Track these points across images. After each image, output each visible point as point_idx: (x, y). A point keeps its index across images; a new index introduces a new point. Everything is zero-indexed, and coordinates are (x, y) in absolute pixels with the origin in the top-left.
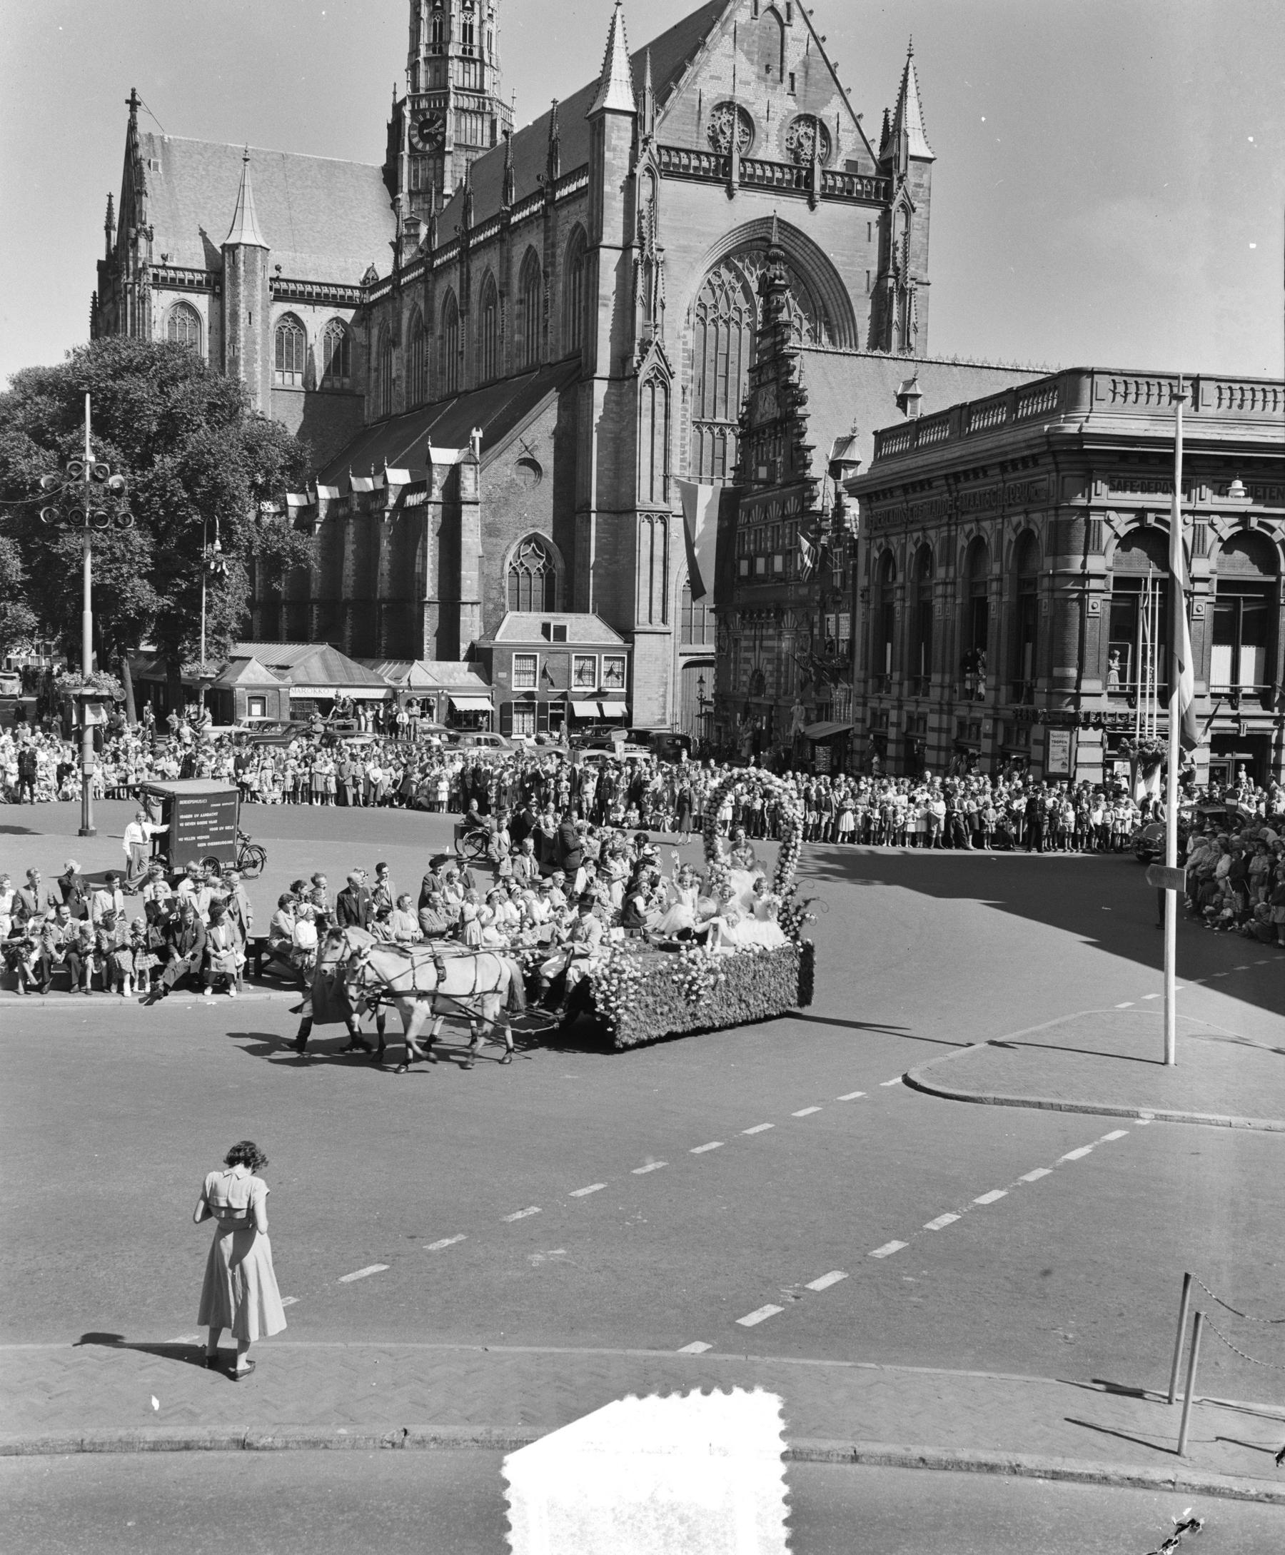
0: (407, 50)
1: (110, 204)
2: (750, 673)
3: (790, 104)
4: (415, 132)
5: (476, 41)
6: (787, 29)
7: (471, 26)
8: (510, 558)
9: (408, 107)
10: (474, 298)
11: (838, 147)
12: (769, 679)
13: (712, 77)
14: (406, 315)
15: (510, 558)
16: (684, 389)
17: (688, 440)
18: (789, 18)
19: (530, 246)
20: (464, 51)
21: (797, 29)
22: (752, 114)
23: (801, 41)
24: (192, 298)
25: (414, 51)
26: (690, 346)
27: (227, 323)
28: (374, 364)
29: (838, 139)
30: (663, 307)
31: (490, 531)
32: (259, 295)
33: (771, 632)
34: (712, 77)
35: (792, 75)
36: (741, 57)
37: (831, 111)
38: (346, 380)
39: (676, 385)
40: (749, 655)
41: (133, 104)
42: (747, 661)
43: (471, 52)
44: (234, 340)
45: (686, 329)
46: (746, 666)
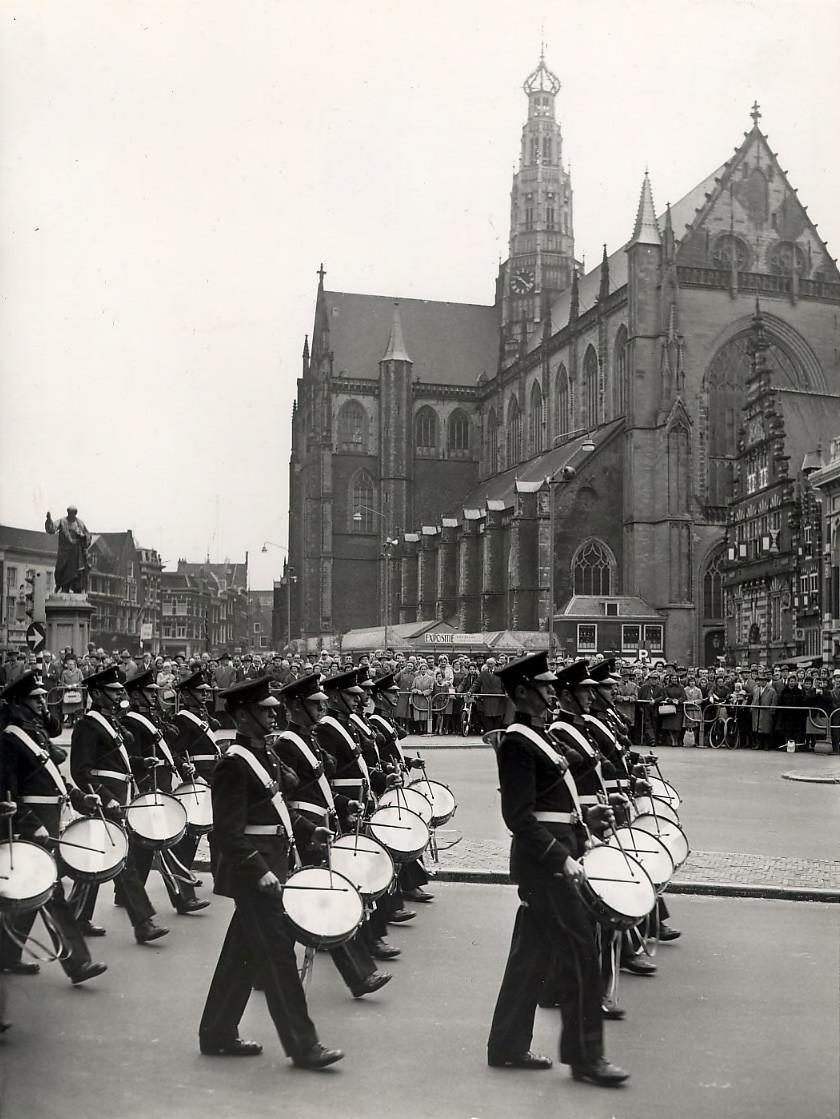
0: (509, 229)
1: (306, 341)
2: (749, 627)
3: (774, 235)
4: (514, 282)
5: (556, 220)
6: (770, 184)
7: (553, 210)
8: (575, 558)
9: (509, 266)
10: (552, 386)
11: (811, 266)
12: (763, 630)
13: (716, 219)
14: (507, 402)
15: (575, 558)
16: (702, 437)
17: (705, 471)
18: (771, 176)
19: (590, 345)
20: (548, 227)
21: (775, 185)
22: (746, 242)
23: (779, 191)
24: (360, 398)
25: (512, 231)
26: (706, 404)
27: (383, 415)
28: (485, 439)
29: (810, 259)
30: (684, 376)
31: (561, 541)
32: (404, 394)
33: (763, 594)
34: (716, 219)
35: (774, 215)
36: (736, 204)
37: (804, 238)
38: (466, 451)
39: (695, 431)
40: (748, 614)
41: (322, 273)
42: (747, 618)
43: (553, 227)
44: (387, 425)
45: (702, 392)
46: (747, 623)
